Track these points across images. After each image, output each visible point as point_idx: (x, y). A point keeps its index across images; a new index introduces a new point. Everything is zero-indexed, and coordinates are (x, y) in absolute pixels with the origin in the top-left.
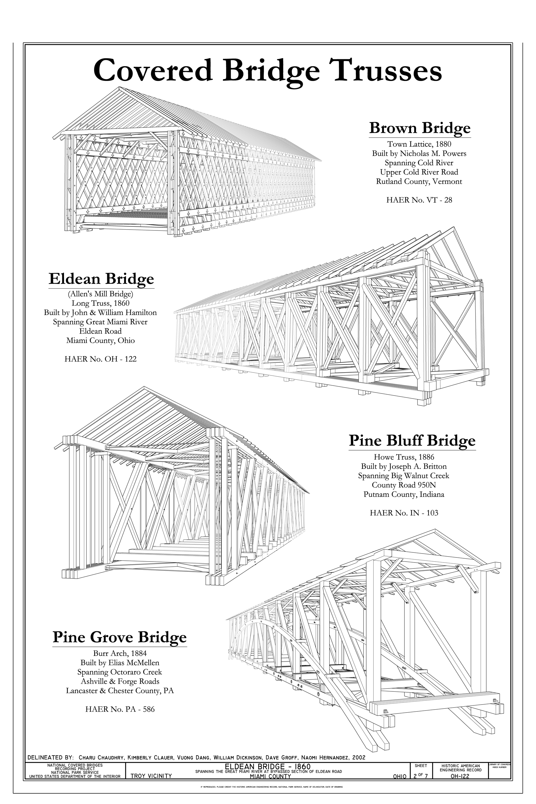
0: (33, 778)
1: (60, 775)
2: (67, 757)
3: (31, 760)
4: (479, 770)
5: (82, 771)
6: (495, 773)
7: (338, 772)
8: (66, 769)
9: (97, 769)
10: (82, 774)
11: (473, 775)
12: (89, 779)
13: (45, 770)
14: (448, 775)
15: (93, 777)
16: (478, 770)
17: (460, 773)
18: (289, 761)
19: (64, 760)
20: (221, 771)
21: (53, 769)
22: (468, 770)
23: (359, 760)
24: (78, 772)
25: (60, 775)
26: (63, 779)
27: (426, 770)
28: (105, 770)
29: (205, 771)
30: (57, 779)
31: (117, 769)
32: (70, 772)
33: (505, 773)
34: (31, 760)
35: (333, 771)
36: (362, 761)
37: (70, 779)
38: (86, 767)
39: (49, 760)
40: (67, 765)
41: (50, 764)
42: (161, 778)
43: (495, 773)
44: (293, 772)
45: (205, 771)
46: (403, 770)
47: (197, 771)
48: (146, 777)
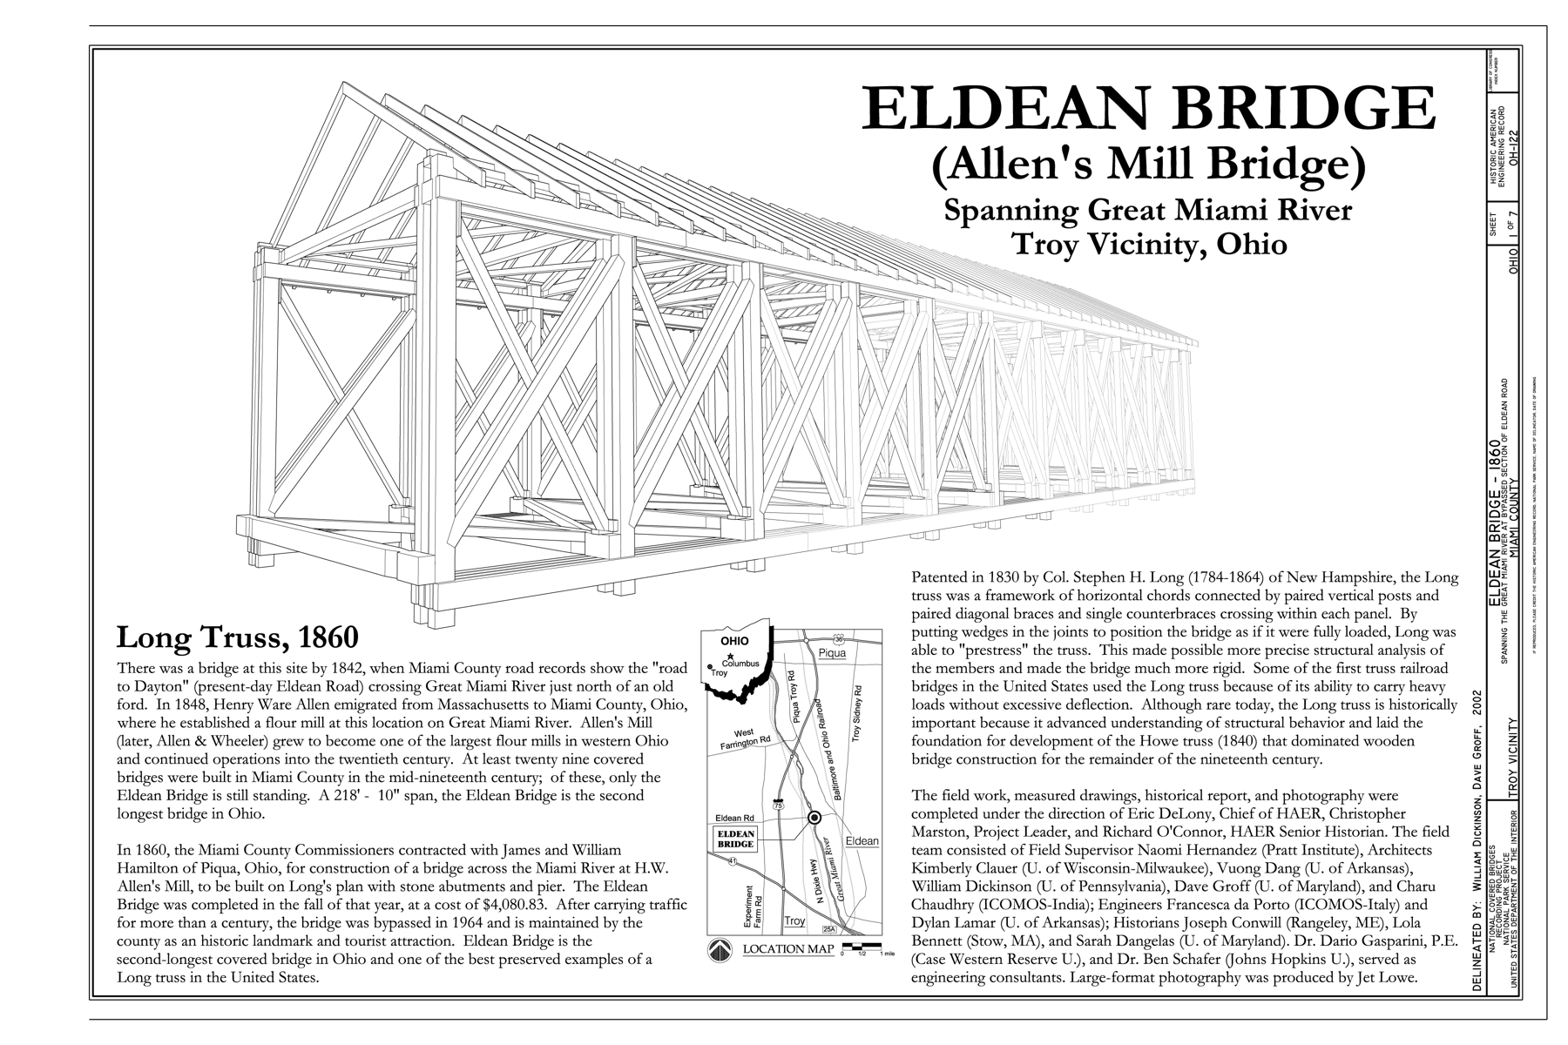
0: (1518, 982)
1: (1511, 928)
2: (1476, 915)
3: (1483, 985)
4: (1502, 110)
5: (1504, 885)
6: (1507, 80)
7: (1505, 385)
8: (1499, 916)
9: (1499, 857)
10: (1509, 885)
11: (1511, 124)
12: (1519, 871)
13: (1501, 957)
14: (1511, 172)
15: (1515, 864)
16: (1501, 113)
17: (1508, 149)
18: (1483, 836)
19: (1482, 921)
20: (1504, 614)
21: (1499, 942)
22: (1501, 133)
23: (1483, 703)
24: (1506, 893)
25: (1511, 928)
26: (1519, 922)
27: (1502, 213)
28: (1502, 842)
29: (1504, 645)
30: (1519, 934)
31: (1500, 816)
32: (1504, 908)
33: (1507, 60)
34: (1483, 985)
35: (1504, 396)
36: (1483, 696)
37: (1519, 908)
38: (1496, 877)
39: (1483, 948)
40: (1491, 915)
41: (1490, 948)
42: (1517, 739)
43: (1507, 80)
44: (1505, 473)
45: (1504, 645)
46: (1501, 258)
47: (1504, 660)
48: (1514, 767)
